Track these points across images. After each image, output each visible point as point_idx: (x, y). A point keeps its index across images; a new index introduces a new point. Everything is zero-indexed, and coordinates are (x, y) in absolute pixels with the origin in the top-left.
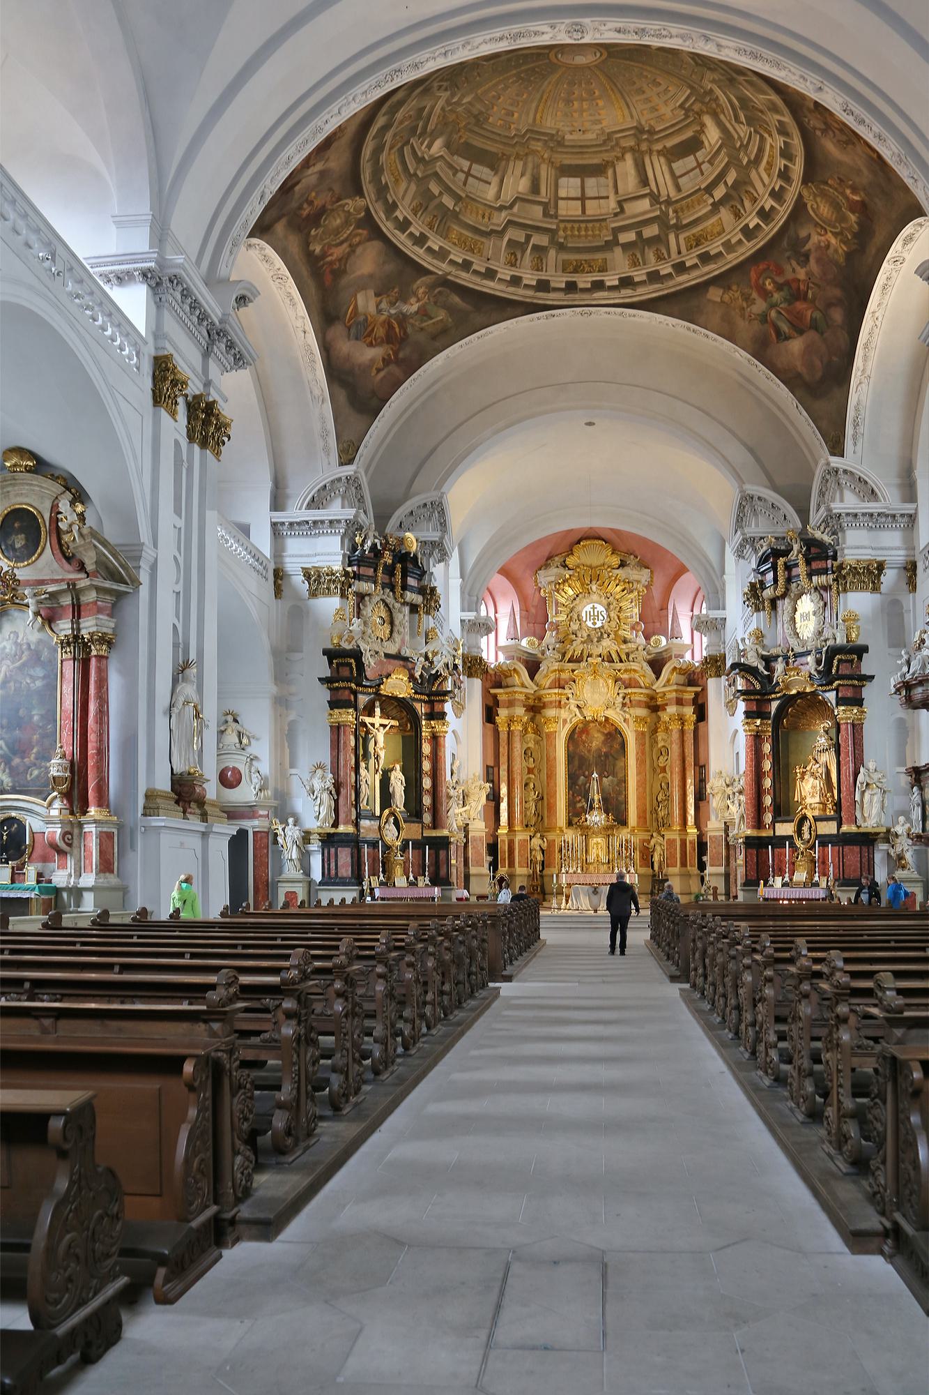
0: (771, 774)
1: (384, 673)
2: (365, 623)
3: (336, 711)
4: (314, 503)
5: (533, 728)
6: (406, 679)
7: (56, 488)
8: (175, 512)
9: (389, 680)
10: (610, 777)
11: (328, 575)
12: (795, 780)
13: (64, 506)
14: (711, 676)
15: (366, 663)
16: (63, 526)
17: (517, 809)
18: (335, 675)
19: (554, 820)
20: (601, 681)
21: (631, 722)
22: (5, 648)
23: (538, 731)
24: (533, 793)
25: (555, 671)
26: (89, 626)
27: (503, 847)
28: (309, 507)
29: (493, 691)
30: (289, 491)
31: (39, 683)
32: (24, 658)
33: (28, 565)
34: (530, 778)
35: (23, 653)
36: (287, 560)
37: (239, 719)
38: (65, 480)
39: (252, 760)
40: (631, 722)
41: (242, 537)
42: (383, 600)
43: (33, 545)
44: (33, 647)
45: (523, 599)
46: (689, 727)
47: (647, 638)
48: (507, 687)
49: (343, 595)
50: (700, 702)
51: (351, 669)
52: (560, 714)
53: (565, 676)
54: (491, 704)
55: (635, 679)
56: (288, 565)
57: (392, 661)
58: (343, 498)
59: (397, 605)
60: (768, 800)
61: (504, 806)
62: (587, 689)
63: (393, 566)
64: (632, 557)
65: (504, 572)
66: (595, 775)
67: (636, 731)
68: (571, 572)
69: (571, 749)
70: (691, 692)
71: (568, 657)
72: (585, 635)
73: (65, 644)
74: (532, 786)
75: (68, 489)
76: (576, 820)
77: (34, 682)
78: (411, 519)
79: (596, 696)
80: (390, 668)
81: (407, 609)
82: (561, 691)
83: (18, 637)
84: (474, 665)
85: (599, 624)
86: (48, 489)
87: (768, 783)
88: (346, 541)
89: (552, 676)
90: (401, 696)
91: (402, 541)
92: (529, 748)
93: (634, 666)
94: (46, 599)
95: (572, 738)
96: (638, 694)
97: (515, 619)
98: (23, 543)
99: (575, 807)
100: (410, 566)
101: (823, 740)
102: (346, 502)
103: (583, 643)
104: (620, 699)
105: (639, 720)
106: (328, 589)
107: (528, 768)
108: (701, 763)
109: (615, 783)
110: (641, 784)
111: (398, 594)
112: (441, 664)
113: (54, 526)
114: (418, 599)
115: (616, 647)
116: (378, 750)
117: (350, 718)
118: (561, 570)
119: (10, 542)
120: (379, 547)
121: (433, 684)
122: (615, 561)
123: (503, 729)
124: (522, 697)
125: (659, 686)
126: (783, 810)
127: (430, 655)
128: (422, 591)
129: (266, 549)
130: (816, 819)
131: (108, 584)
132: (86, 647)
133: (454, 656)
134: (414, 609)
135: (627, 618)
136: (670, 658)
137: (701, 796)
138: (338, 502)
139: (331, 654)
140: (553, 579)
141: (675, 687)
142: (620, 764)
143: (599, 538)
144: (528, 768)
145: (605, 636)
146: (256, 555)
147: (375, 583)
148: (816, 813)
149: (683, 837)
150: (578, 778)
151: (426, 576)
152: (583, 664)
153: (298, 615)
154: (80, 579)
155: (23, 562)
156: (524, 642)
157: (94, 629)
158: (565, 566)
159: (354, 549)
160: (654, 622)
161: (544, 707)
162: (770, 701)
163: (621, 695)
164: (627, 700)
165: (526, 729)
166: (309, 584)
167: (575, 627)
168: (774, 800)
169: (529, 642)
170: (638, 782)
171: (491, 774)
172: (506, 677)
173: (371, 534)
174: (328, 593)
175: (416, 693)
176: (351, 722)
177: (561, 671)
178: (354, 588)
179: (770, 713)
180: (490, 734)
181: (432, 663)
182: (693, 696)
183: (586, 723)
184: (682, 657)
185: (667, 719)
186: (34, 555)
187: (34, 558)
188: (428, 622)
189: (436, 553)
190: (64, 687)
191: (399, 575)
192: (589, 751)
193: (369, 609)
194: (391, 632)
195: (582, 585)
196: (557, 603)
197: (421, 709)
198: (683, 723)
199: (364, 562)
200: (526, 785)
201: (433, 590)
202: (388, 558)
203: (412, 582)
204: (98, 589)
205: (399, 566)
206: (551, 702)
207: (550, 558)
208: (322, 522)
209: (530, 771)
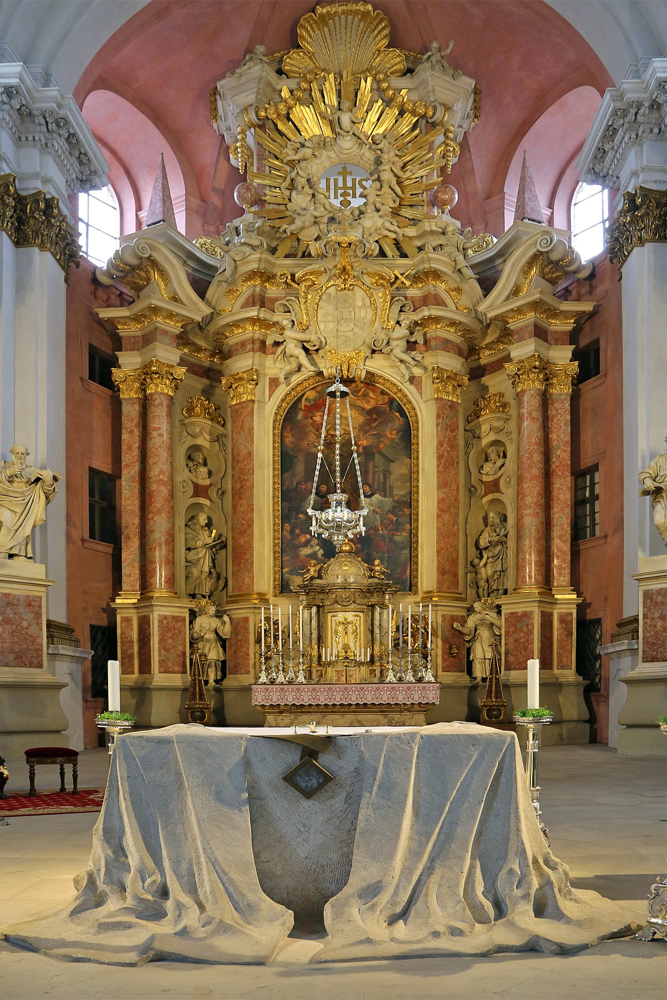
19: (247, 580)
20: (359, 293)
24: (206, 533)
34: (199, 506)
52: (263, 365)
62: (326, 308)
69: (289, 440)
76: (297, 581)
89: (246, 289)
99: (296, 556)
107: (196, 486)
109: (388, 507)
110: (446, 507)
142: (399, 469)
144: (196, 486)
170: (441, 501)
198: (547, 380)
209: (199, 491)
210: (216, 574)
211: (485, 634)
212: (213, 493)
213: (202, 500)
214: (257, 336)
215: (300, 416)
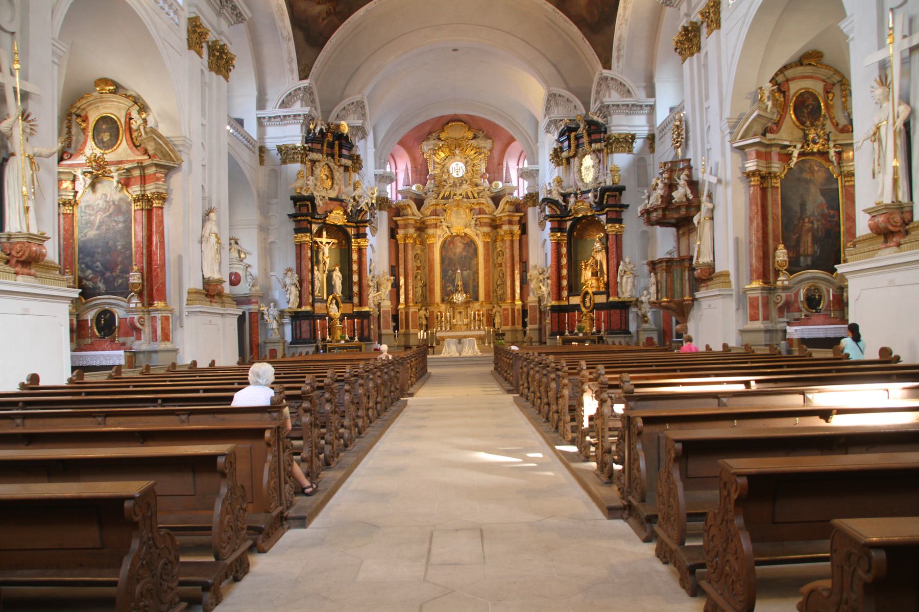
0: (566, 267)
1: (329, 209)
2: (316, 179)
3: (300, 235)
4: (284, 104)
5: (419, 241)
6: (342, 213)
7: (129, 103)
8: (202, 116)
9: (332, 214)
10: (468, 271)
11: (293, 149)
12: (581, 270)
13: (134, 114)
14: (530, 206)
15: (317, 204)
16: (134, 126)
17: (411, 292)
18: (298, 212)
20: (462, 211)
21: (480, 236)
22: (99, 204)
23: (423, 243)
25: (433, 205)
26: (150, 189)
27: (402, 317)
28: (279, 108)
29: (395, 219)
30: (268, 97)
31: (121, 225)
32: (111, 210)
33: (112, 151)
34: (418, 273)
35: (110, 207)
36: (267, 141)
37: (239, 242)
38: (134, 97)
39: (247, 267)
40: (480, 236)
41: (239, 127)
42: (327, 164)
43: (115, 137)
44: (116, 203)
45: (413, 159)
46: (517, 238)
47: (490, 183)
48: (404, 215)
49: (302, 162)
50: (523, 222)
51: (308, 208)
52: (436, 232)
53: (439, 208)
54: (394, 227)
55: (483, 209)
56: (268, 144)
57: (334, 202)
58: (302, 100)
59: (336, 167)
60: (565, 283)
61: (402, 291)
63: (333, 141)
64: (481, 132)
65: (402, 143)
66: (459, 271)
67: (484, 241)
68: (443, 143)
69: (443, 254)
70: (518, 216)
71: (441, 196)
72: (452, 182)
73: (136, 200)
74: (419, 277)
75: (136, 103)
77: (117, 225)
78: (344, 112)
79: (459, 221)
80: (332, 207)
81: (342, 168)
82: (437, 217)
83: (107, 197)
84: (383, 203)
85: (460, 175)
86: (123, 104)
87: (564, 272)
88: (304, 127)
89: (432, 208)
90: (339, 224)
91: (338, 126)
92: (417, 254)
93: (482, 200)
94: (124, 172)
95: (444, 246)
96: (485, 218)
97: (408, 173)
98: (109, 138)
100: (344, 142)
101: (598, 245)
102: (304, 103)
103: (450, 187)
104: (473, 222)
105: (486, 234)
106: (293, 158)
107: (417, 266)
108: (524, 260)
110: (487, 275)
111: (336, 160)
112: (364, 203)
113: (128, 126)
114: (349, 163)
115: (471, 189)
116: (325, 258)
117: (308, 239)
118: (436, 141)
119: (100, 138)
120: (325, 131)
121: (359, 216)
122: (470, 135)
123: (401, 242)
124: (413, 222)
125: (497, 213)
126: (574, 289)
127: (357, 198)
128: (351, 157)
129: (254, 135)
130: (594, 294)
131: (163, 162)
132: (149, 201)
133: (372, 198)
134: (346, 169)
135: (477, 170)
136: (504, 195)
137: (524, 282)
138: (298, 103)
139: (297, 200)
140: (431, 147)
141: (508, 213)
143: (460, 121)
144: (417, 266)
145: (464, 182)
146: (248, 138)
147: (322, 153)
148: (594, 290)
149: (513, 307)
150: (448, 272)
151: (354, 149)
152: (450, 200)
153: (275, 174)
154: (145, 160)
155: (108, 150)
156: (414, 188)
157: (154, 191)
158: (439, 139)
159: (309, 132)
160: (494, 173)
161: (426, 228)
162: (566, 221)
163: (474, 219)
164: (478, 222)
165: (415, 242)
166: (281, 155)
167: (445, 177)
168: (568, 282)
169: (418, 188)
170: (485, 273)
171: (394, 271)
172: (403, 209)
173: (319, 123)
174: (293, 161)
175: (348, 222)
176: (308, 241)
177: (437, 205)
178: (309, 157)
179: (566, 228)
180: (393, 245)
181: (358, 202)
182: (518, 218)
183: (453, 237)
184: (512, 194)
185: (503, 233)
186: (115, 145)
187: (115, 147)
188: (355, 177)
189: (360, 134)
190: (137, 227)
191: (337, 148)
192: (455, 255)
193: (319, 170)
194: (333, 184)
195: (450, 150)
196: (434, 162)
197: (352, 232)
199: (314, 140)
200: (416, 277)
201: (358, 156)
202: (330, 138)
203: (345, 152)
204: (157, 165)
205: (337, 142)
206: (431, 225)
207: (430, 133)
208: (289, 116)
209: (418, 268)
210: (424, 296)
211: (498, 314)
212: (422, 268)
213: (419, 271)
214: (435, 222)
215: (446, 245)
